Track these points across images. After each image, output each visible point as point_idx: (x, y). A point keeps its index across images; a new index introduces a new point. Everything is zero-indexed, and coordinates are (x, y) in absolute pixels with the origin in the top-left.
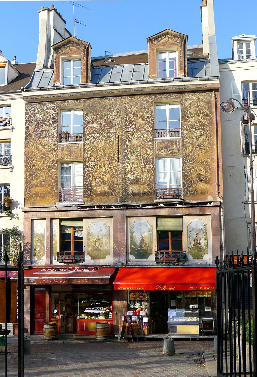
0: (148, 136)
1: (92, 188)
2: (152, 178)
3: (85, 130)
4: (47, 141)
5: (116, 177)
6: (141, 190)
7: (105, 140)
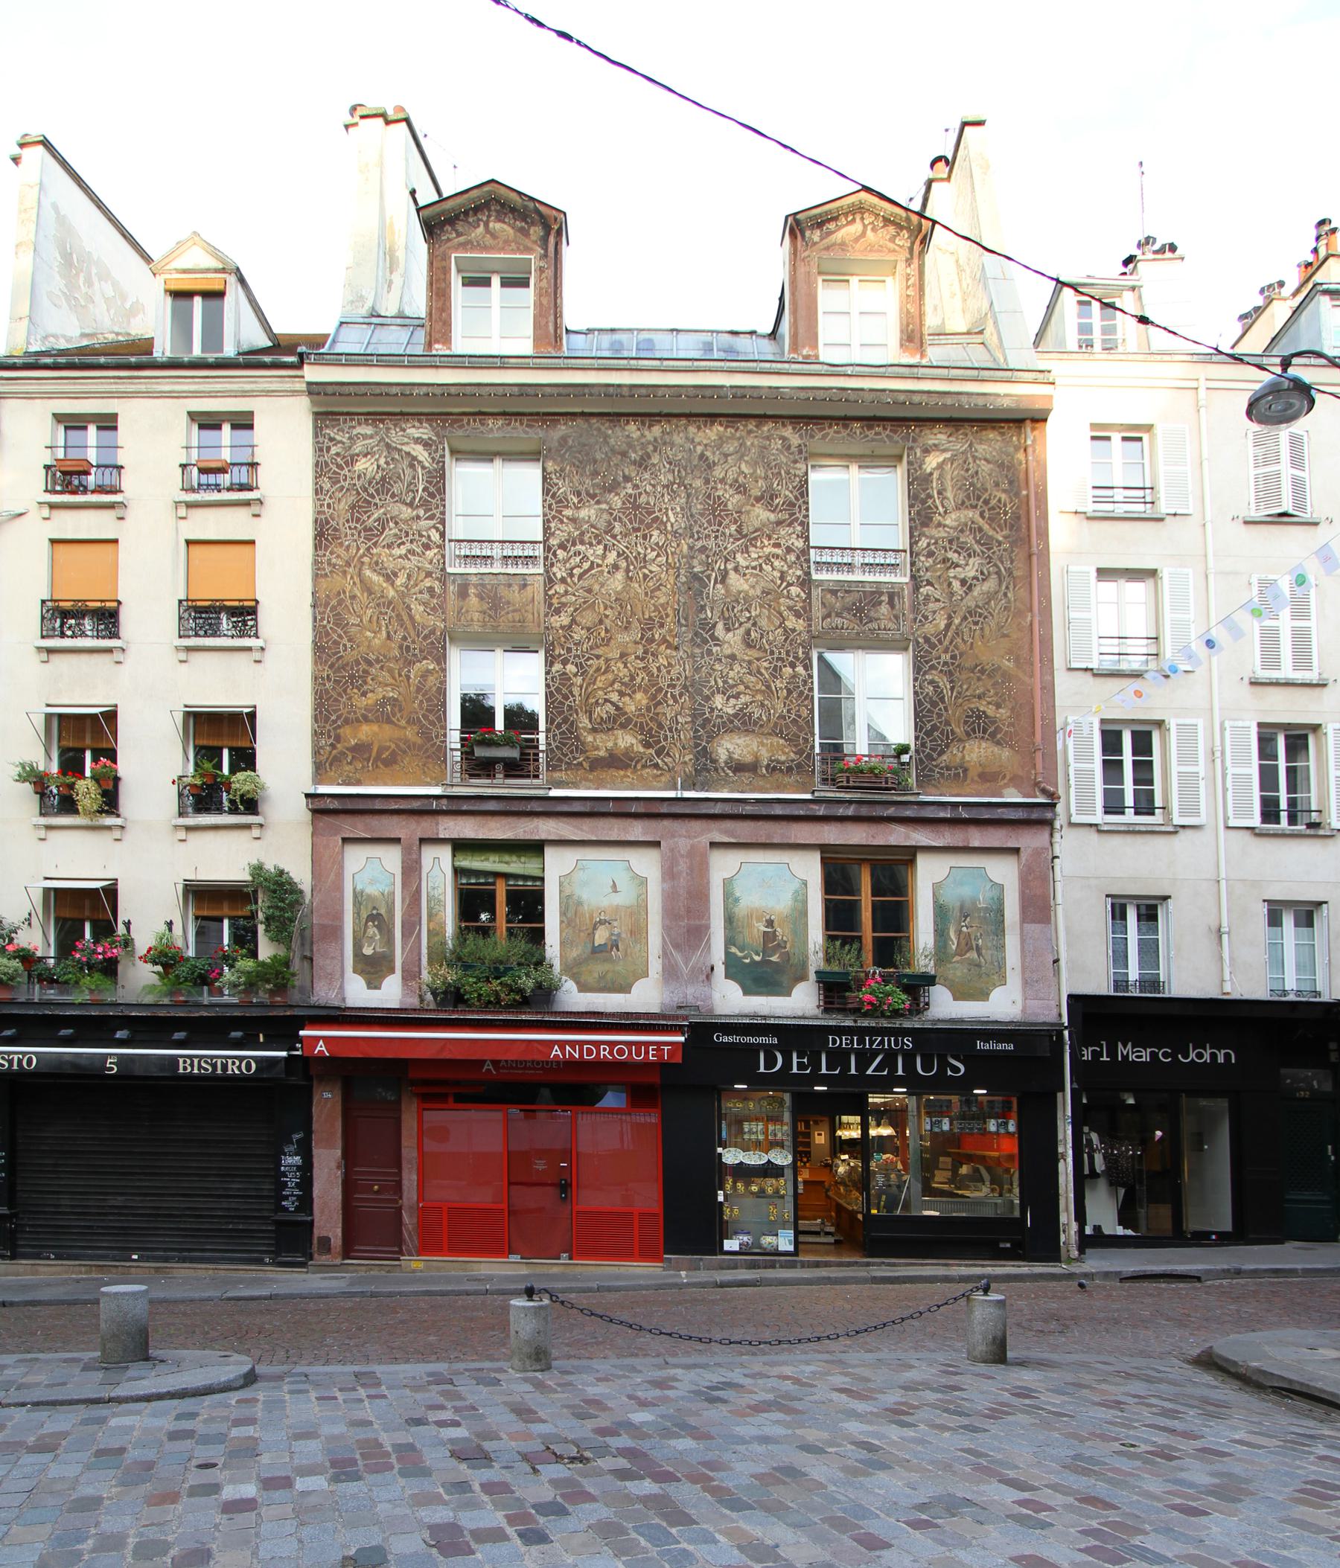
0: (790, 567)
3: (549, 528)
4: (400, 557)
5: (671, 702)
6: (765, 756)
7: (627, 571)
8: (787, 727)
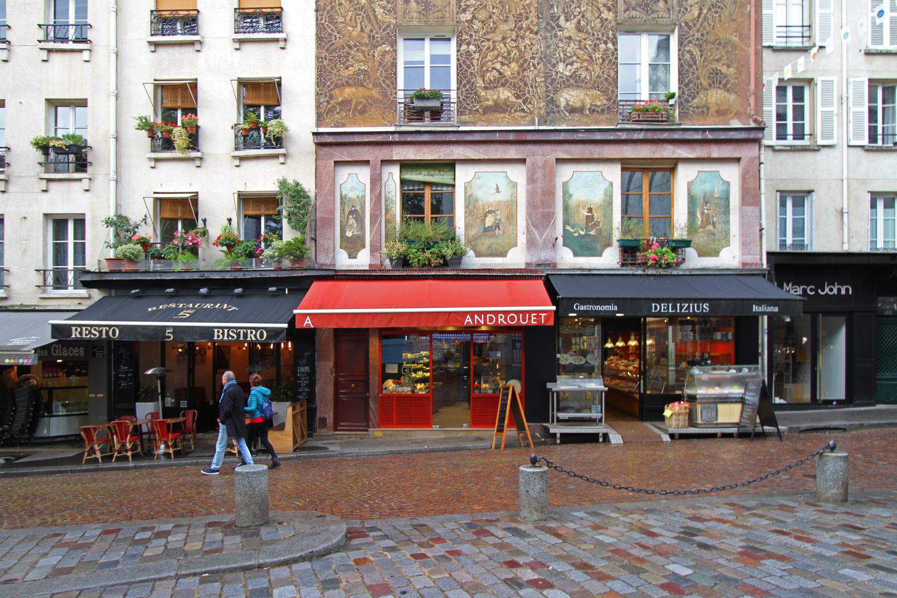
1: (476, 94)
2: (612, 73)
5: (532, 68)
6: (588, 101)
8: (602, 83)
